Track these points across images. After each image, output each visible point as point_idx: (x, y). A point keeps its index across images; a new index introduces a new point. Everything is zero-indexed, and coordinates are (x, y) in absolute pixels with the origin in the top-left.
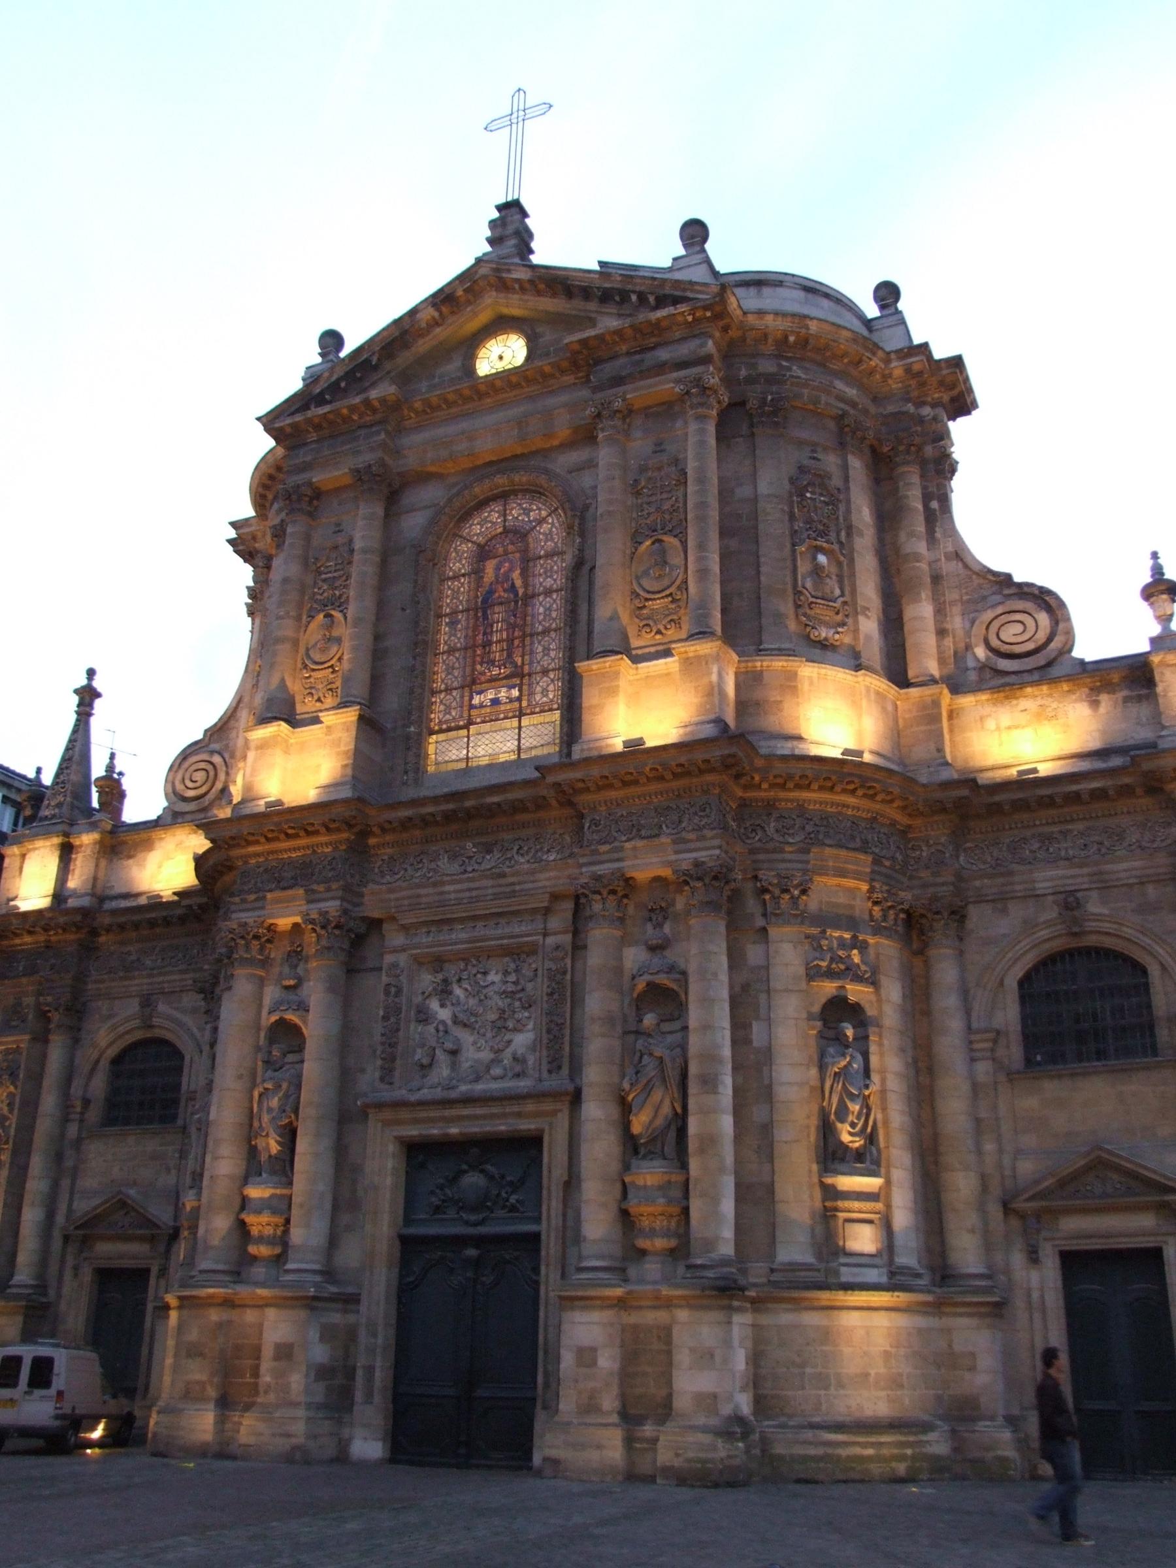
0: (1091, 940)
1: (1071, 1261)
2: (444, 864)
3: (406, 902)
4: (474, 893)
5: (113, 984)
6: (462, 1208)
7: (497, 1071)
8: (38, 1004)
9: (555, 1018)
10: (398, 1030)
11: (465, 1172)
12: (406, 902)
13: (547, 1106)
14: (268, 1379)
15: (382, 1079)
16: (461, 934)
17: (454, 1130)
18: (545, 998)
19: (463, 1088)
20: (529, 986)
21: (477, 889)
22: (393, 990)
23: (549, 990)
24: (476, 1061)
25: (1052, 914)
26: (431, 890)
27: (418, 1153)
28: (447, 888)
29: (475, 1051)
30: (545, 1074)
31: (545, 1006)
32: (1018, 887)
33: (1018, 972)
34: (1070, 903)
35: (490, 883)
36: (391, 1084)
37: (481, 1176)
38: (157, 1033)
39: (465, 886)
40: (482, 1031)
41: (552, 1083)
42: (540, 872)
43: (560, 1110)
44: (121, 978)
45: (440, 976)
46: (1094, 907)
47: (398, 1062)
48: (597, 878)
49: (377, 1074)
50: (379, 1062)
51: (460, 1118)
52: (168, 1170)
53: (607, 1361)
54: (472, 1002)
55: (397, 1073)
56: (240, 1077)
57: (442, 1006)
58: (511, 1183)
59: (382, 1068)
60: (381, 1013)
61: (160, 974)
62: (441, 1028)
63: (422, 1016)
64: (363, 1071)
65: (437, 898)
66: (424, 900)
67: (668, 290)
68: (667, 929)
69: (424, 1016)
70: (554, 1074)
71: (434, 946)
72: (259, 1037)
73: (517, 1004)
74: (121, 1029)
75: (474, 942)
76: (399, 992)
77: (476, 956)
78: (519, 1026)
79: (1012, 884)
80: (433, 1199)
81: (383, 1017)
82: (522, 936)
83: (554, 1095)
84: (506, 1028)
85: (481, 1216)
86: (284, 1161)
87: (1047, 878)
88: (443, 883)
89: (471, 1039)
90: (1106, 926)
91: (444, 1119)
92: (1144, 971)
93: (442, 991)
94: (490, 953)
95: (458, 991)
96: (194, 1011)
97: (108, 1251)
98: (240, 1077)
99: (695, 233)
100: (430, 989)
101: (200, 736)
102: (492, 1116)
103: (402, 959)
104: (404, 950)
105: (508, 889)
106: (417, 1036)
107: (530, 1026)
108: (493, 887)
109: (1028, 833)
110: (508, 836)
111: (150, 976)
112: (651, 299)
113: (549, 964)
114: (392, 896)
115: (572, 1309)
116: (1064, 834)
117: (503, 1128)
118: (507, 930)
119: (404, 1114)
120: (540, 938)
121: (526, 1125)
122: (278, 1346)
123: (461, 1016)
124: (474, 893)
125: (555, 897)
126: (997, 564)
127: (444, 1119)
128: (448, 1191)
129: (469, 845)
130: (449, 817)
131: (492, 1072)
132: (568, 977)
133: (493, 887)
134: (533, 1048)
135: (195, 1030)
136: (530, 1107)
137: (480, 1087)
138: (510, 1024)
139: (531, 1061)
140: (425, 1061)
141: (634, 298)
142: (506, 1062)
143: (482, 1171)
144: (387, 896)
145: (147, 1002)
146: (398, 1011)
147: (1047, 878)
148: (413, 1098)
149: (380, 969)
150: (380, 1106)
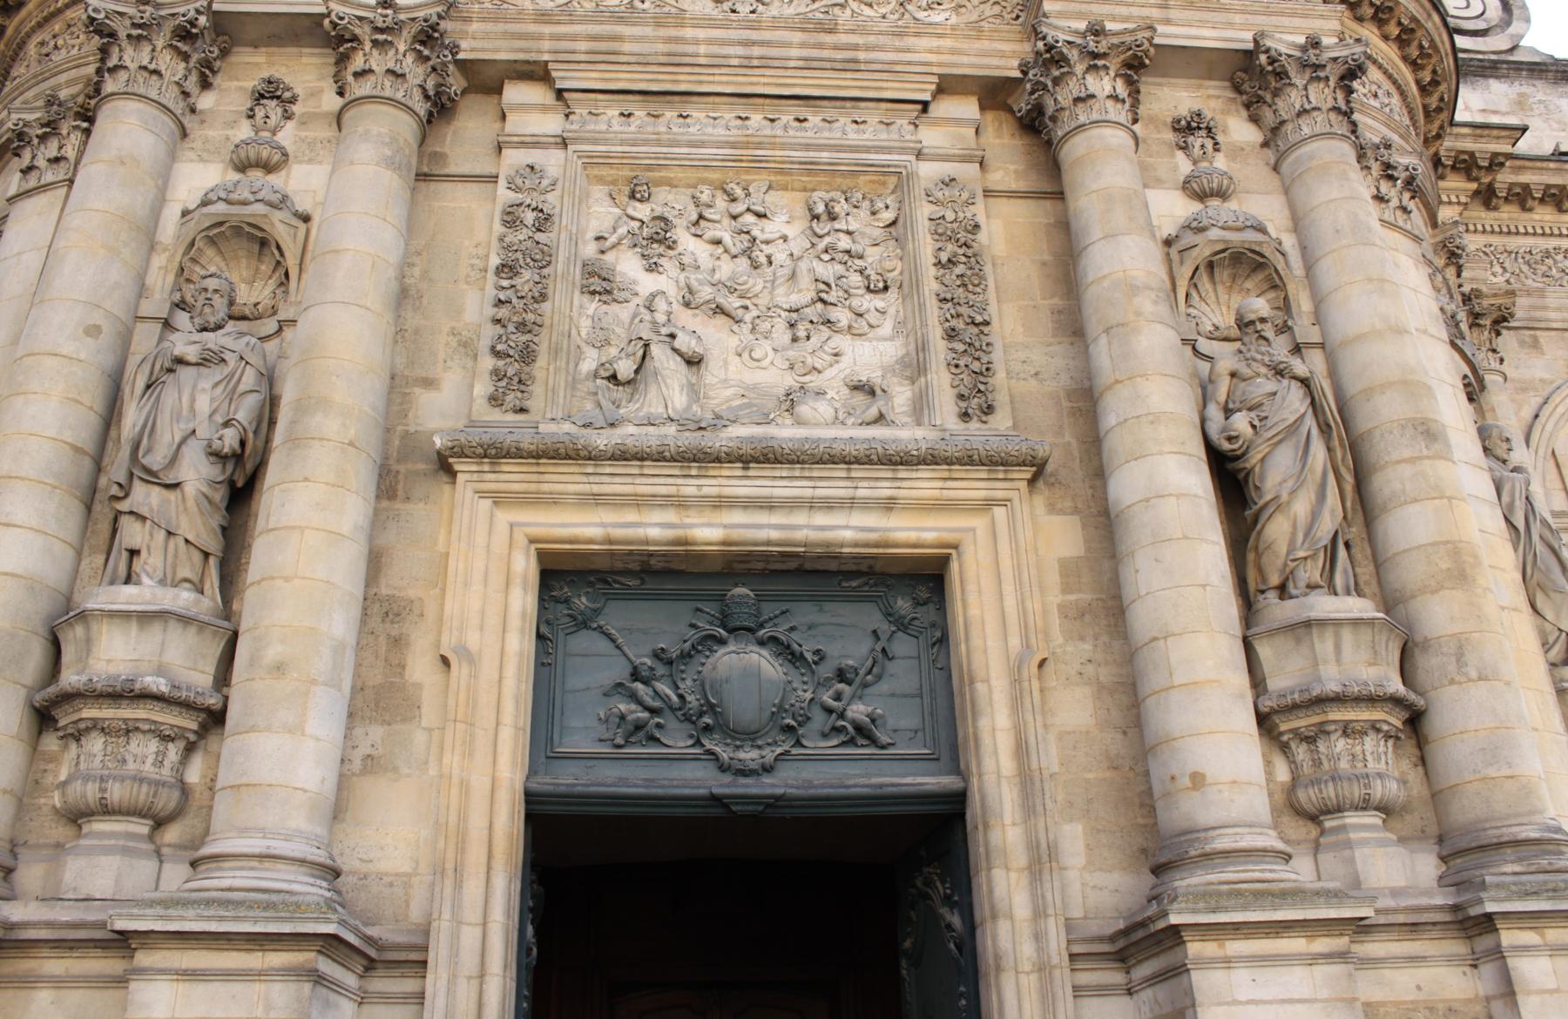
3: (583, 46)
4: (757, 51)
6: (707, 729)
9: (963, 310)
10: (543, 297)
11: (722, 642)
12: (583, 46)
13: (973, 486)
15: (495, 400)
16: (710, 127)
17: (707, 532)
18: (933, 271)
20: (873, 255)
21: (762, 43)
22: (529, 217)
23: (944, 257)
24: (754, 387)
26: (648, 31)
27: (573, 585)
28: (689, 33)
31: (935, 286)
32: (1552, 315)
35: (798, 37)
36: (522, 410)
37: (765, 652)
40: (764, 326)
41: (977, 435)
42: (917, 35)
43: (1003, 503)
45: (642, 211)
47: (541, 362)
49: (483, 388)
50: (488, 362)
54: (726, 269)
55: (537, 389)
56: (93, 331)
57: (653, 268)
58: (841, 675)
59: (498, 375)
60: (495, 261)
62: (661, 305)
63: (596, 284)
64: (429, 383)
65: (661, 47)
66: (627, 47)
70: (974, 425)
71: (646, 142)
72: (148, 261)
73: (855, 279)
75: (746, 145)
76: (544, 221)
77: (736, 175)
78: (861, 325)
79: (1545, 308)
80: (623, 707)
81: (499, 270)
82: (868, 150)
83: (995, 462)
84: (828, 322)
85: (769, 755)
86: (206, 555)
89: (733, 342)
93: (652, 240)
98: (93, 331)
100: (622, 230)
103: (552, 161)
104: (564, 143)
105: (840, 55)
106: (585, 324)
107: (887, 328)
108: (803, 45)
109: (1552, 243)
114: (547, 29)
115: (1228, 962)
117: (848, 535)
118: (832, 135)
119: (568, 480)
120: (913, 158)
121: (910, 531)
123: (706, 293)
124: (757, 51)
125: (948, 86)
128: (664, 688)
131: (804, 410)
132: (982, 237)
133: (803, 45)
134: (915, 367)
136: (924, 484)
137: (785, 432)
138: (842, 316)
139: (901, 396)
140: (625, 368)
142: (831, 394)
143: (761, 643)
144: (533, 28)
146: (543, 260)
148: (602, 440)
149: (493, 179)
150: (494, 454)
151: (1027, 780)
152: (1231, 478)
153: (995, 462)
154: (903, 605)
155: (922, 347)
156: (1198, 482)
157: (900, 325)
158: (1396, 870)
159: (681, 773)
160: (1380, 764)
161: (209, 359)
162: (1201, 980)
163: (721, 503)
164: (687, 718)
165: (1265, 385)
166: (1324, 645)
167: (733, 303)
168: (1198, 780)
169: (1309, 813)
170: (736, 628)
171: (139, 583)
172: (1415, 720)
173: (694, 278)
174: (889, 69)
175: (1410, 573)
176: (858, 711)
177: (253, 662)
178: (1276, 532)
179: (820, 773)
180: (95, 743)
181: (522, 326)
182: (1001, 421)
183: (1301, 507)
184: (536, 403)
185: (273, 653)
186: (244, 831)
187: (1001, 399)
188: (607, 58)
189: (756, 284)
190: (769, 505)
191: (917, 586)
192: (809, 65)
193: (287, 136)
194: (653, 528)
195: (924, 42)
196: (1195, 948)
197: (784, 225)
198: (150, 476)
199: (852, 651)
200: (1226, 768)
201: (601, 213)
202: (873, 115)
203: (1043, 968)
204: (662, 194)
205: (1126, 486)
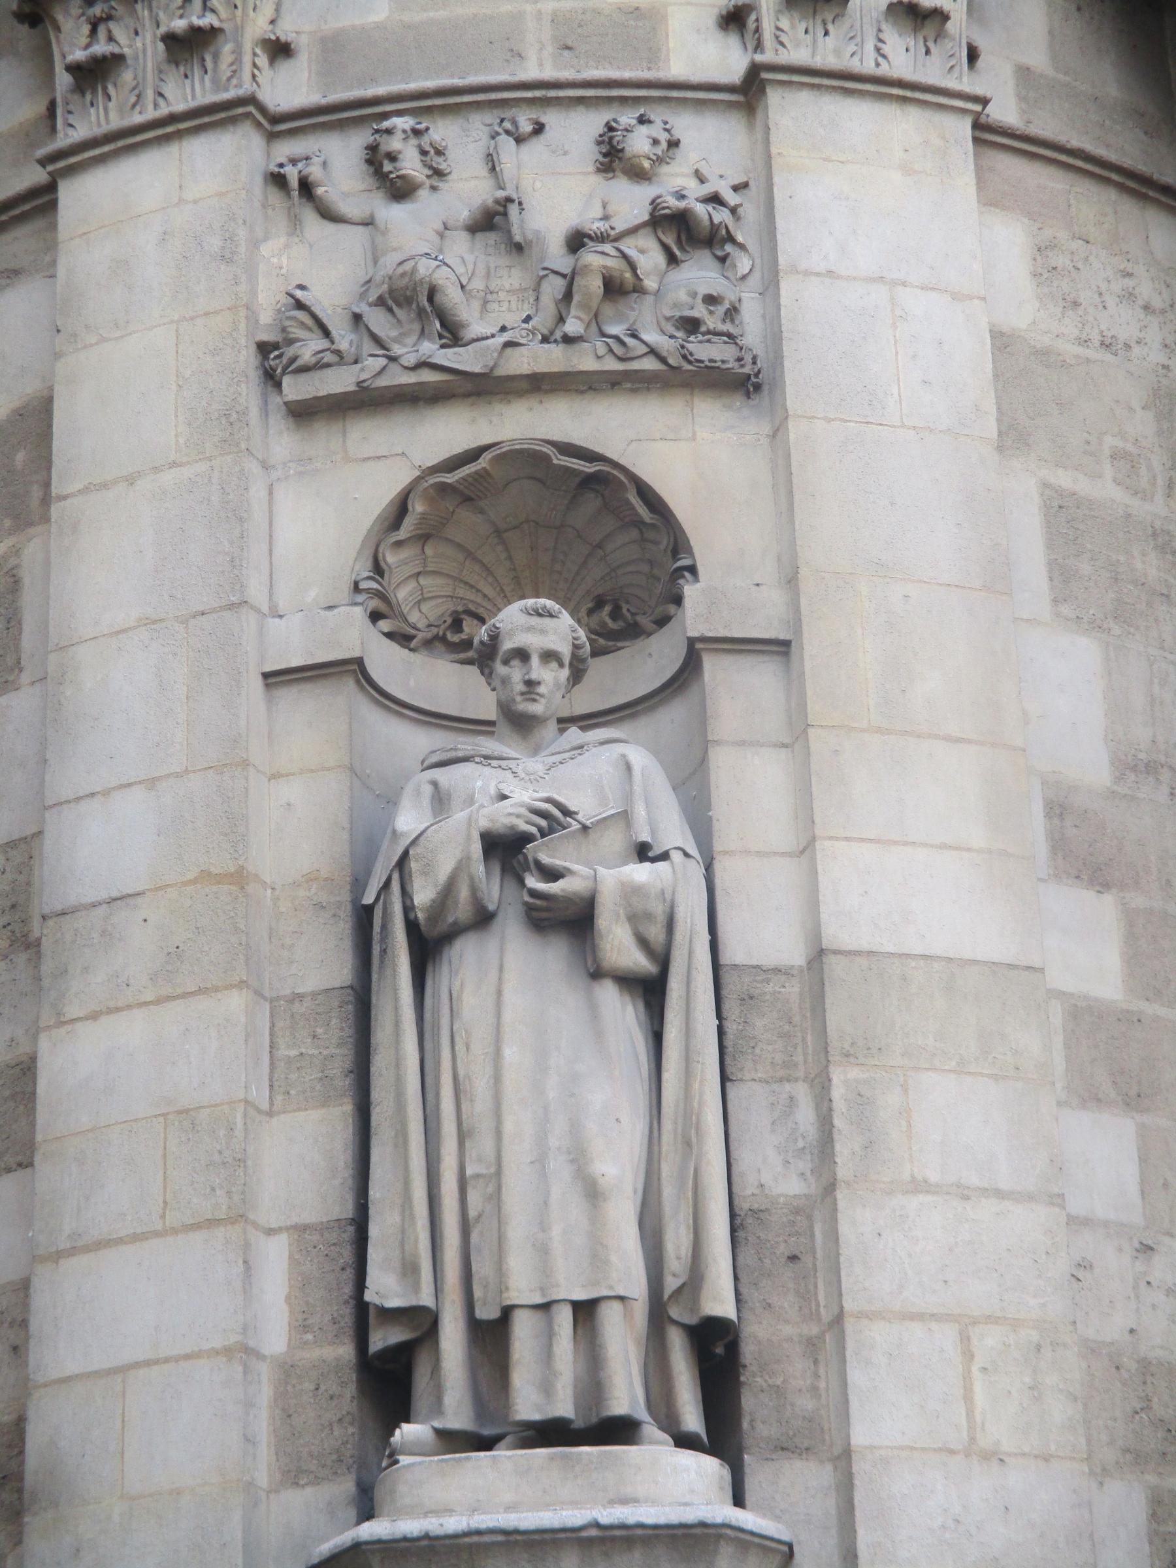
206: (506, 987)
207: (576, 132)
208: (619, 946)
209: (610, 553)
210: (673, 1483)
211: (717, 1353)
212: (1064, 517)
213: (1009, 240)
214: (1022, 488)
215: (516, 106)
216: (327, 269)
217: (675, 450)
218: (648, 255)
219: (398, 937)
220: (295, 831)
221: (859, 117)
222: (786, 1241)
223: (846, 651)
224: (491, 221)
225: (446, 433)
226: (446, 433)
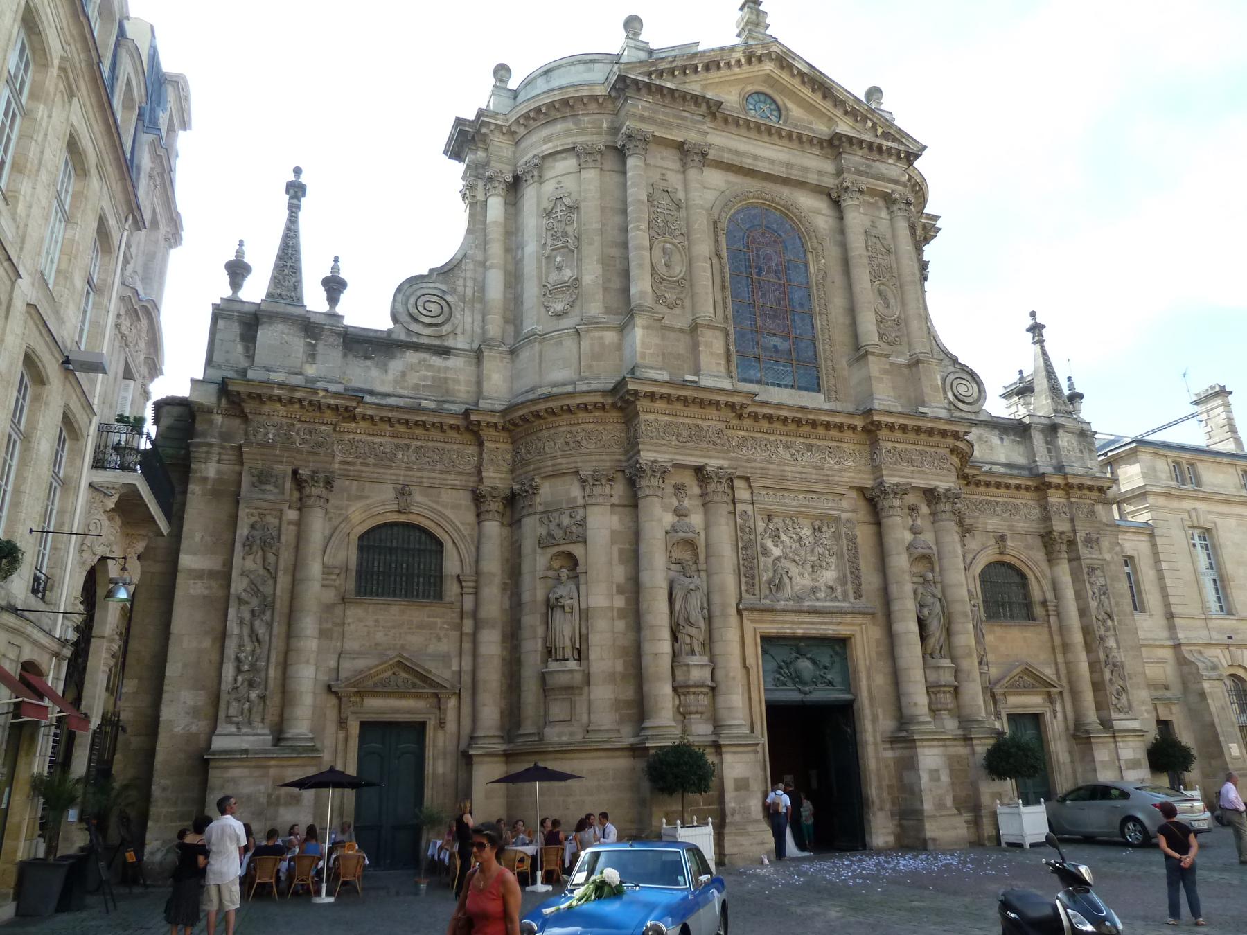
0: (1007, 559)
1: (1011, 717)
2: (781, 449)
5: (364, 469)
7: (822, 595)
8: (295, 472)
13: (859, 620)
14: (733, 805)
15: (747, 591)
16: (789, 502)
17: (800, 632)
19: (807, 603)
25: (992, 542)
28: (787, 468)
29: (800, 580)
30: (852, 600)
33: (978, 570)
34: (1002, 538)
38: (412, 519)
39: (800, 469)
44: (375, 466)
46: (1009, 543)
48: (897, 485)
51: (802, 623)
52: (439, 639)
53: (945, 778)
55: (757, 587)
57: (776, 546)
61: (419, 470)
67: (892, 131)
68: (919, 522)
69: (766, 552)
74: (376, 511)
87: (994, 523)
88: (784, 464)
90: (1015, 553)
91: (792, 622)
92: (1023, 576)
94: (807, 516)
95: (784, 537)
96: (455, 507)
97: (379, 706)
99: (874, 93)
101: (426, 272)
102: (822, 623)
103: (749, 508)
110: (819, 443)
111: (408, 469)
112: (880, 131)
113: (844, 530)
116: (997, 503)
119: (768, 616)
121: (844, 631)
122: (736, 780)
125: (851, 487)
126: (953, 350)
127: (792, 622)
129: (798, 441)
130: (798, 422)
134: (842, 581)
135: (458, 524)
136: (848, 619)
137: (818, 604)
138: (824, 564)
141: (869, 124)
145: (403, 492)
147: (994, 523)
151: (871, 699)
152: (922, 624)
153: (864, 614)
154: (837, 648)
155: (845, 576)
156: (914, 627)
157: (837, 566)
158: (951, 725)
159: (790, 695)
160: (947, 699)
161: (697, 589)
162: (919, 751)
163: (802, 623)
164: (792, 679)
165: (930, 600)
166: (941, 672)
167: (797, 559)
168: (916, 704)
169: (933, 711)
170: (800, 654)
171: (693, 653)
172: (956, 689)
173: (788, 550)
174: (837, 484)
175: (959, 652)
176: (829, 677)
177: (727, 676)
178: (932, 642)
179: (820, 694)
180: (692, 697)
181: (751, 568)
182: (863, 599)
183: (937, 635)
184: (757, 592)
185: (731, 674)
186: (734, 719)
187: (863, 592)
188: (764, 475)
189: (802, 553)
190: (812, 623)
191: (841, 644)
192: (817, 481)
193: (686, 502)
194: (787, 630)
195: (846, 474)
196: (918, 744)
197: (806, 532)
198: (691, 625)
199: (826, 661)
200: (919, 699)
201: (761, 525)
202: (830, 497)
203: (875, 744)
204: (776, 520)
205: (899, 627)
206: (558, 614)
207: (568, 512)
208: (567, 609)
209: (572, 561)
210: (572, 664)
211: (579, 651)
212: (621, 552)
213: (615, 518)
214: (615, 549)
215: (561, 511)
216: (543, 531)
217: (577, 550)
218: (574, 529)
219: (551, 606)
220: (540, 595)
221: (596, 509)
222: (584, 638)
223: (593, 574)
224: (558, 525)
225: (556, 549)
226: (556, 549)
